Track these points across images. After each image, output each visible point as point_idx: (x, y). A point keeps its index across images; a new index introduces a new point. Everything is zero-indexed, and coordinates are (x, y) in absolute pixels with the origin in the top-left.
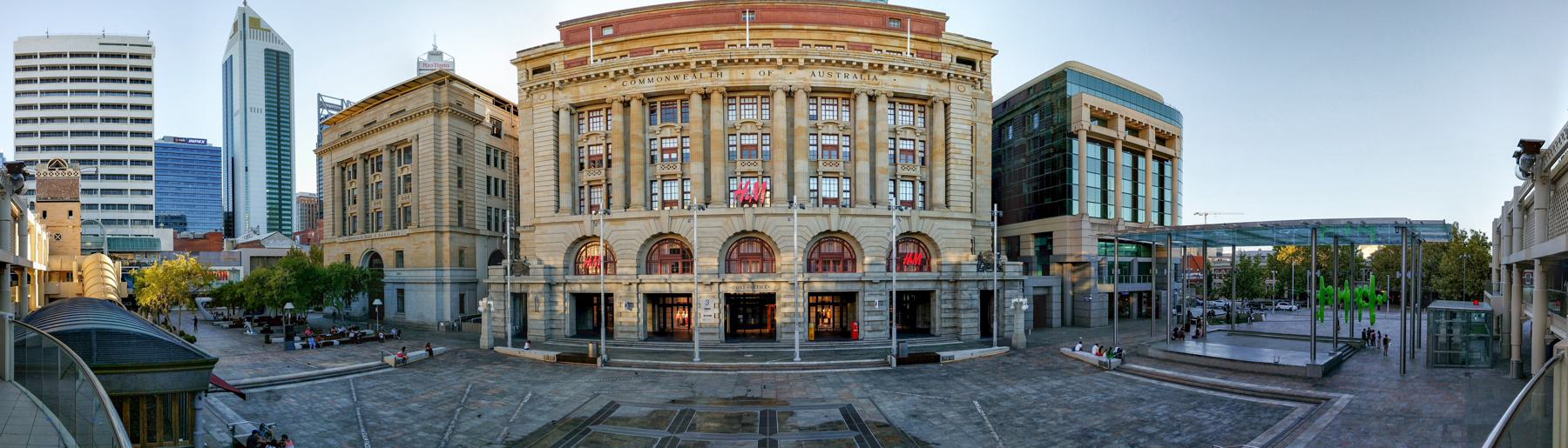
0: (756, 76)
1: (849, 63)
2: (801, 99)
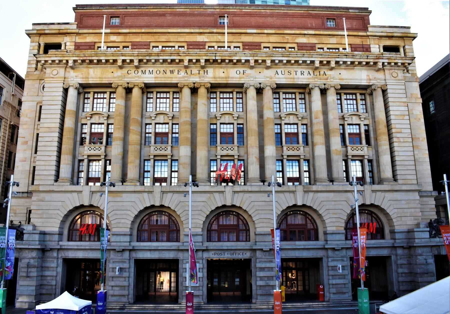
0: (233, 75)
2: (268, 94)
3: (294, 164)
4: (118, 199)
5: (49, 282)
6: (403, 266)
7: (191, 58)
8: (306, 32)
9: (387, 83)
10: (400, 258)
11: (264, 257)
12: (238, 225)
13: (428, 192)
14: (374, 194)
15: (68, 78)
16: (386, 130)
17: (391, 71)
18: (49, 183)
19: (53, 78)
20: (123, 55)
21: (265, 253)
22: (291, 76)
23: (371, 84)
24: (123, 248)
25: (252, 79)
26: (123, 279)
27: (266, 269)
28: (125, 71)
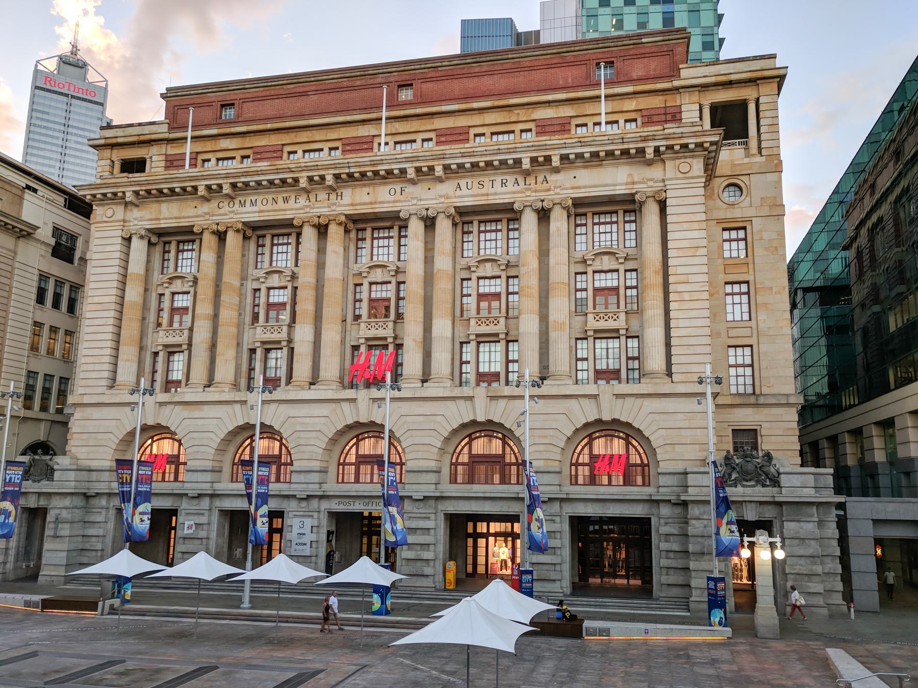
1: (503, 163)
2: (444, 227)
3: (493, 349)
4: (197, 414)
5: (92, 546)
6: (671, 538)
7: (310, 174)
8: (550, 97)
9: (668, 187)
10: (666, 523)
11: (416, 510)
12: (503, 456)
13: (780, 397)
14: (620, 401)
15: (130, 221)
16: (659, 279)
17: (678, 162)
18: (100, 390)
19: (106, 222)
20: (204, 178)
21: (417, 504)
22: (484, 191)
23: (634, 191)
24: (199, 492)
25: (415, 202)
26: (199, 542)
27: (419, 532)
28: (214, 204)
